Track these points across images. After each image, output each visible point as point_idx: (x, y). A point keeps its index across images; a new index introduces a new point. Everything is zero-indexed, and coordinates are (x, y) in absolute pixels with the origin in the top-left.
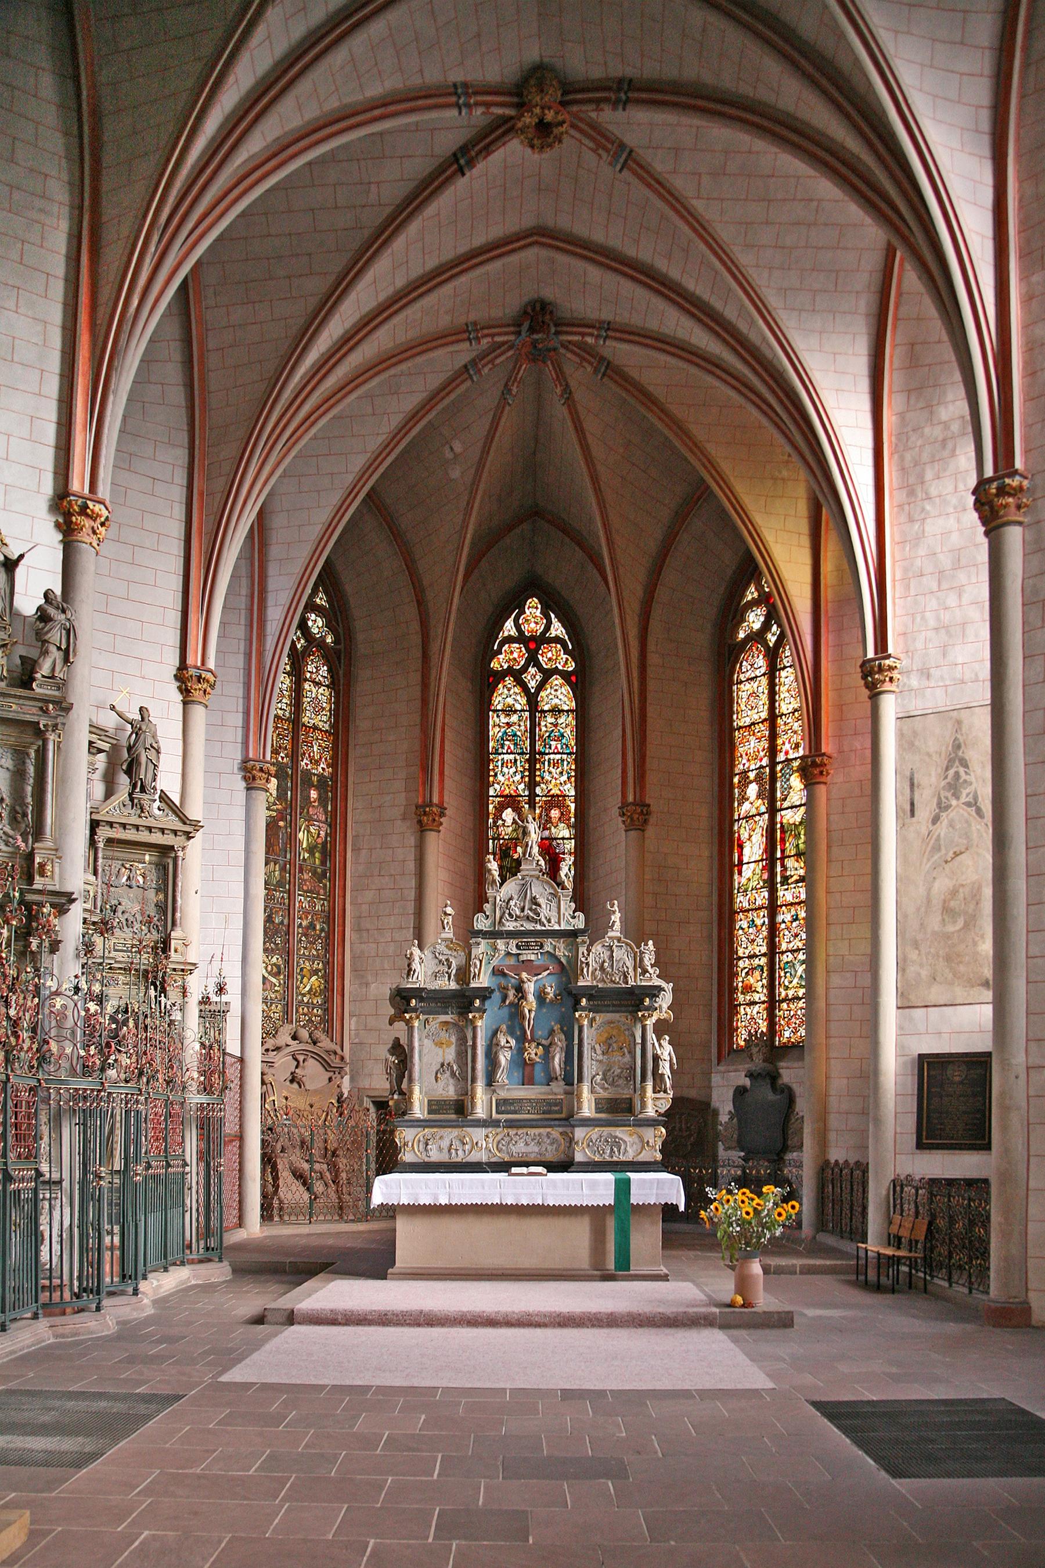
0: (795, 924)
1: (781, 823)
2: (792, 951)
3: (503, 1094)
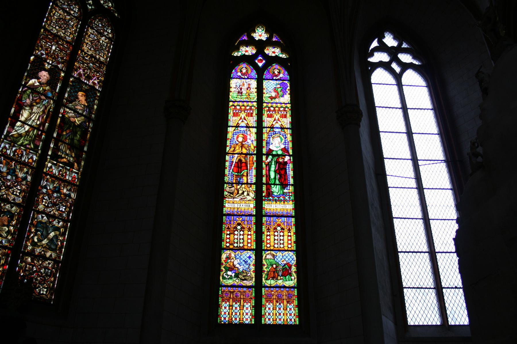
0: (55, 195)
1: (63, 117)
2: (48, 215)
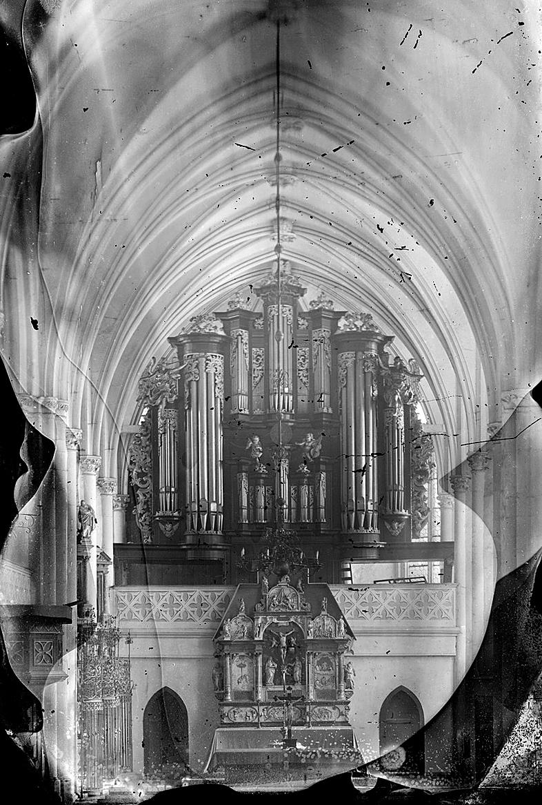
3: (271, 689)
